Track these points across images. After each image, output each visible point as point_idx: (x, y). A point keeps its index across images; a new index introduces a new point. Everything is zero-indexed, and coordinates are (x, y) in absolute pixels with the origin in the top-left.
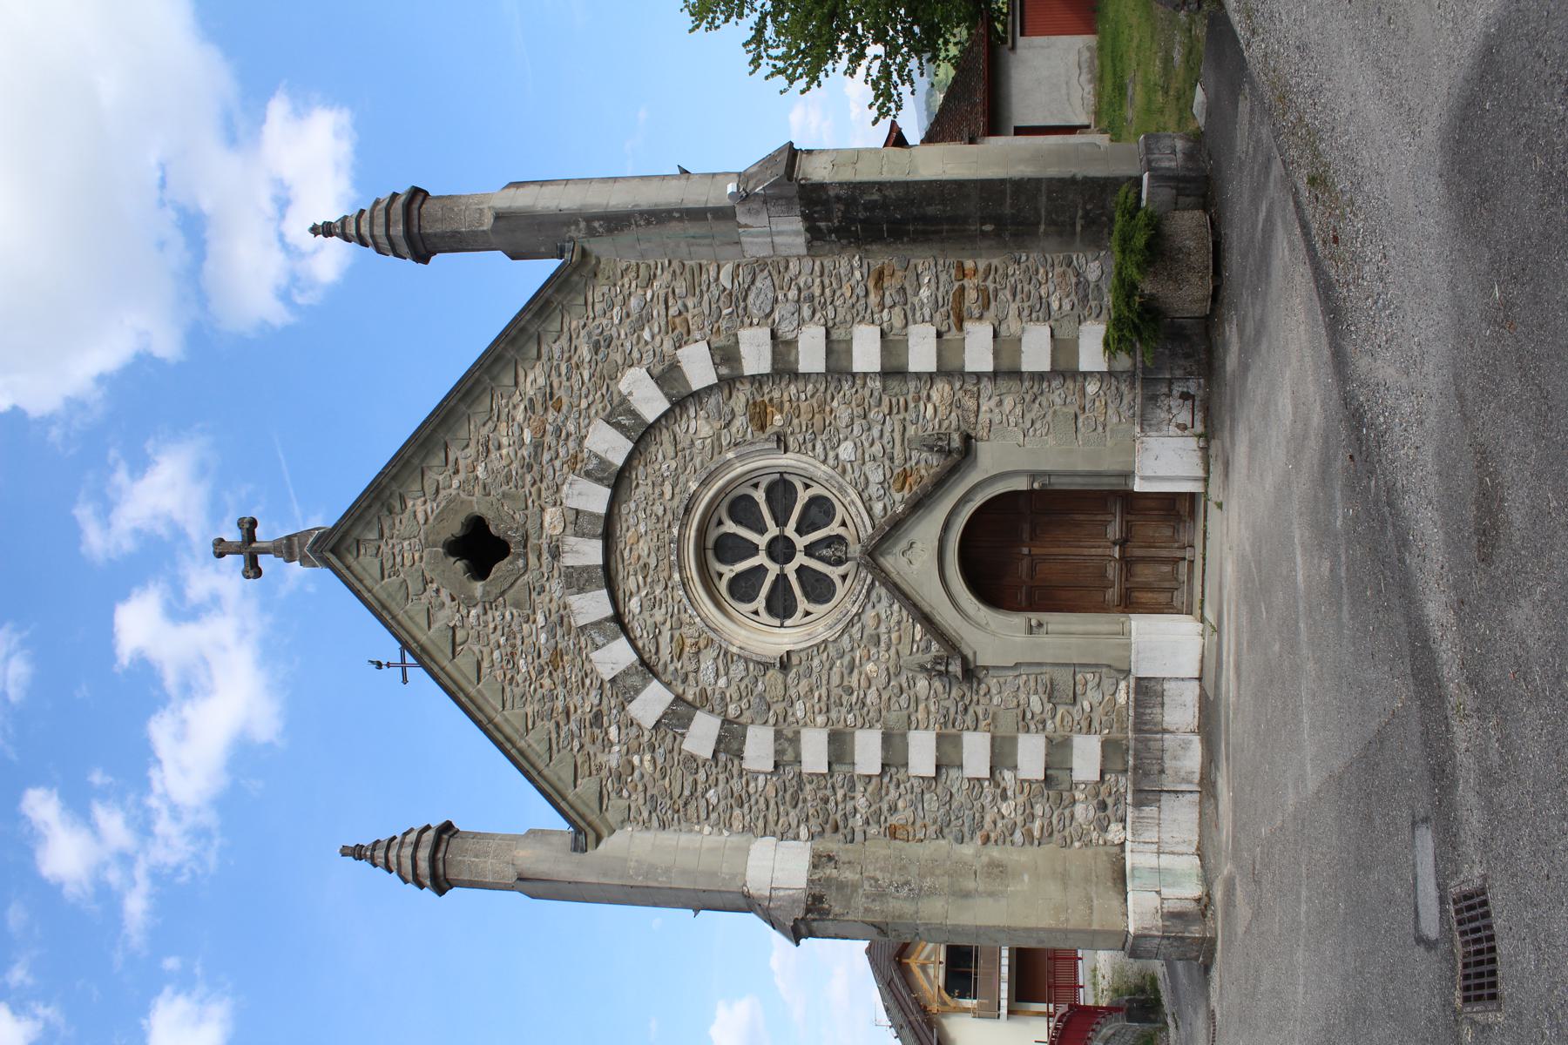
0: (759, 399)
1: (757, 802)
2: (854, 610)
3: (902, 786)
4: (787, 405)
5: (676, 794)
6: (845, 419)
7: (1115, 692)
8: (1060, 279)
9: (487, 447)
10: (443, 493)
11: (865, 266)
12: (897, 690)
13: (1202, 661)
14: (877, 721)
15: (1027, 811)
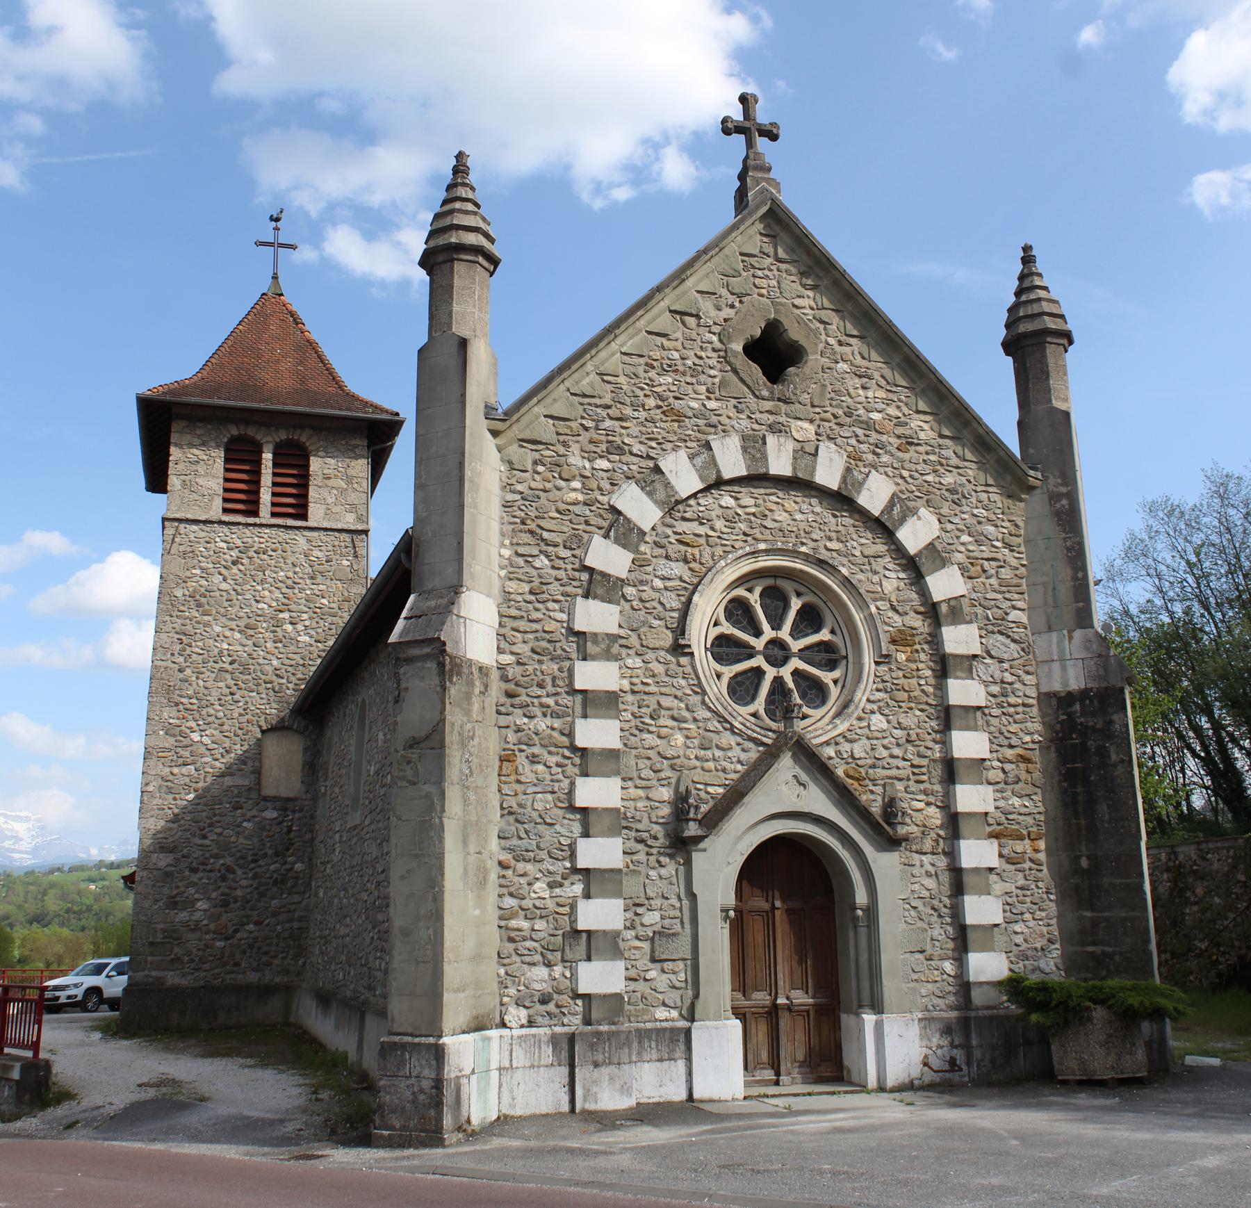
2: (736, 724)
11: (1031, 746)
12: (658, 766)
15: (538, 912)
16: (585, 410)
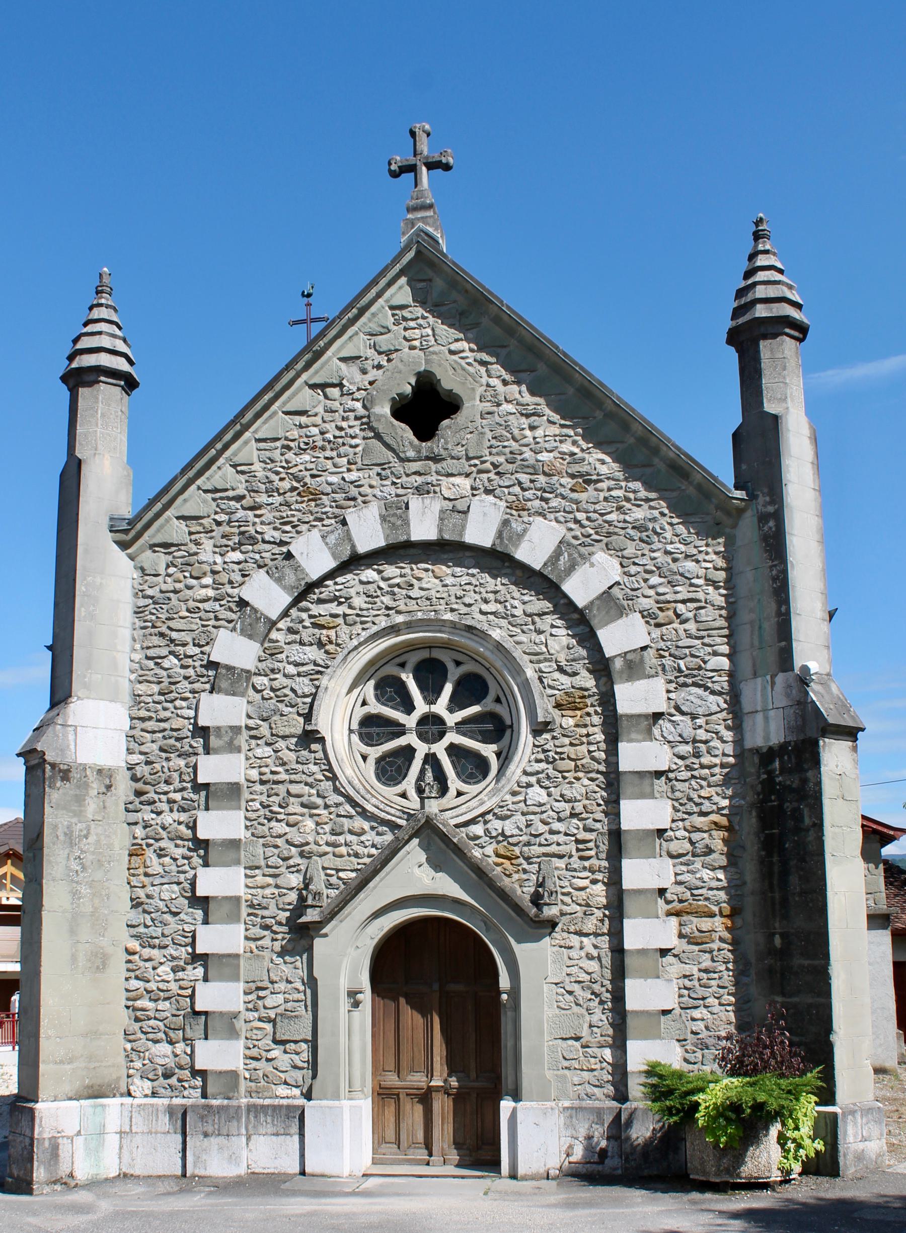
1: (165, 709)
2: (369, 807)
3: (186, 861)
4: (584, 731)
5: (171, 624)
6: (568, 794)
7: (288, 1084)
8: (724, 1019)
10: (483, 370)
12: (286, 854)
13: (323, 1176)
14: (253, 835)
15: (162, 994)
16: (218, 506)
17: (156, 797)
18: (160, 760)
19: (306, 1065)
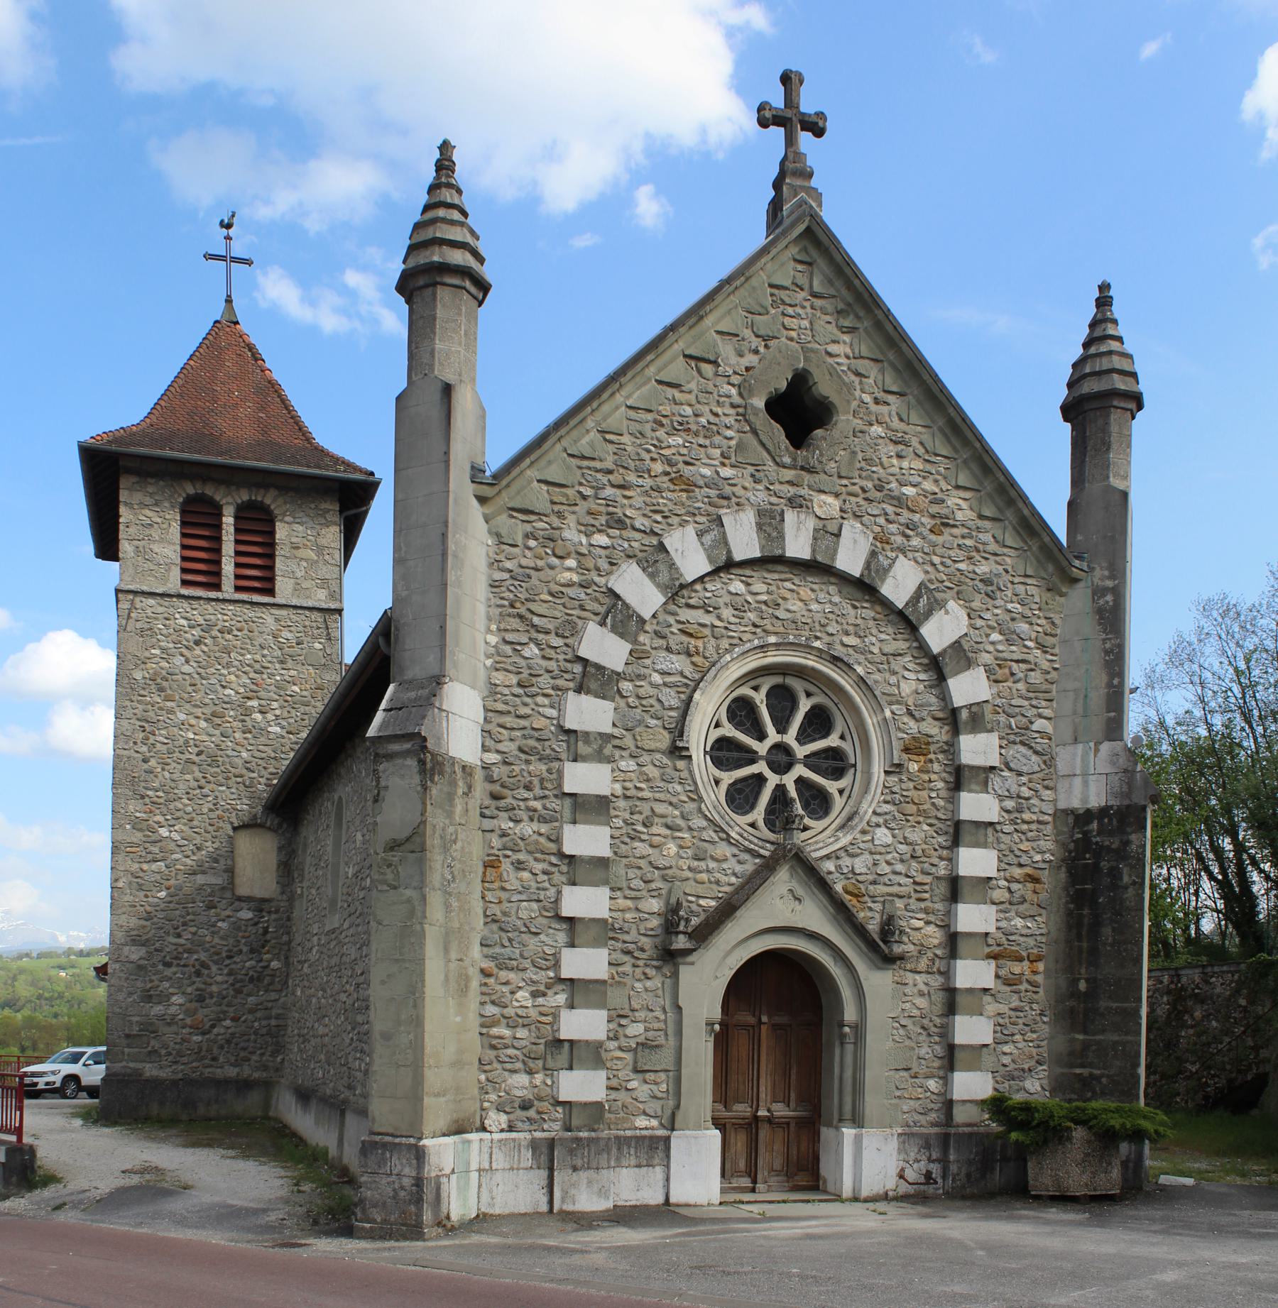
0: (932, 748)
2: (733, 834)
3: (546, 877)
4: (926, 777)
9: (900, 443)
10: (857, 380)
11: (1043, 866)
12: (649, 876)
17: (515, 803)
18: (518, 762)
19: (664, 1095)
